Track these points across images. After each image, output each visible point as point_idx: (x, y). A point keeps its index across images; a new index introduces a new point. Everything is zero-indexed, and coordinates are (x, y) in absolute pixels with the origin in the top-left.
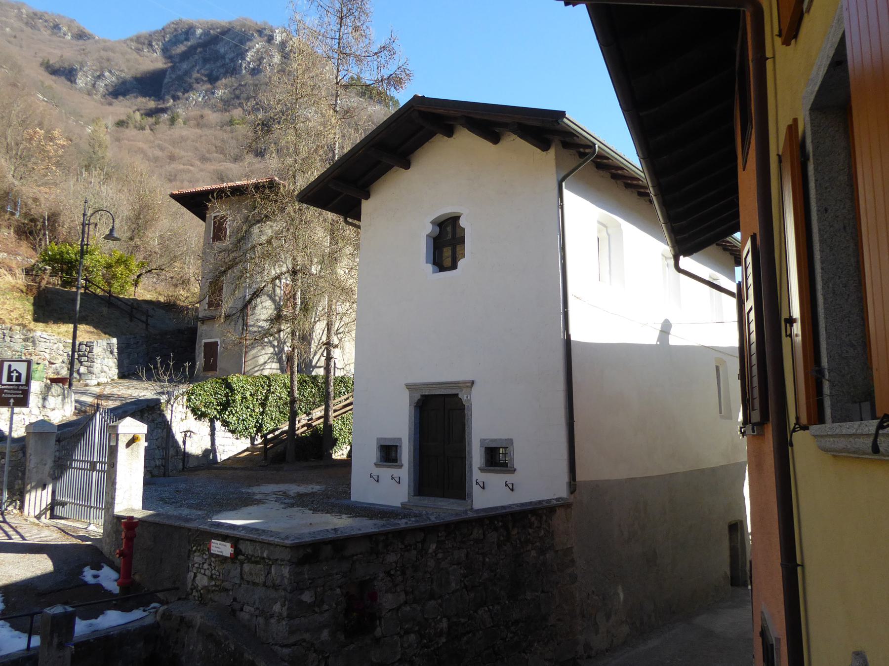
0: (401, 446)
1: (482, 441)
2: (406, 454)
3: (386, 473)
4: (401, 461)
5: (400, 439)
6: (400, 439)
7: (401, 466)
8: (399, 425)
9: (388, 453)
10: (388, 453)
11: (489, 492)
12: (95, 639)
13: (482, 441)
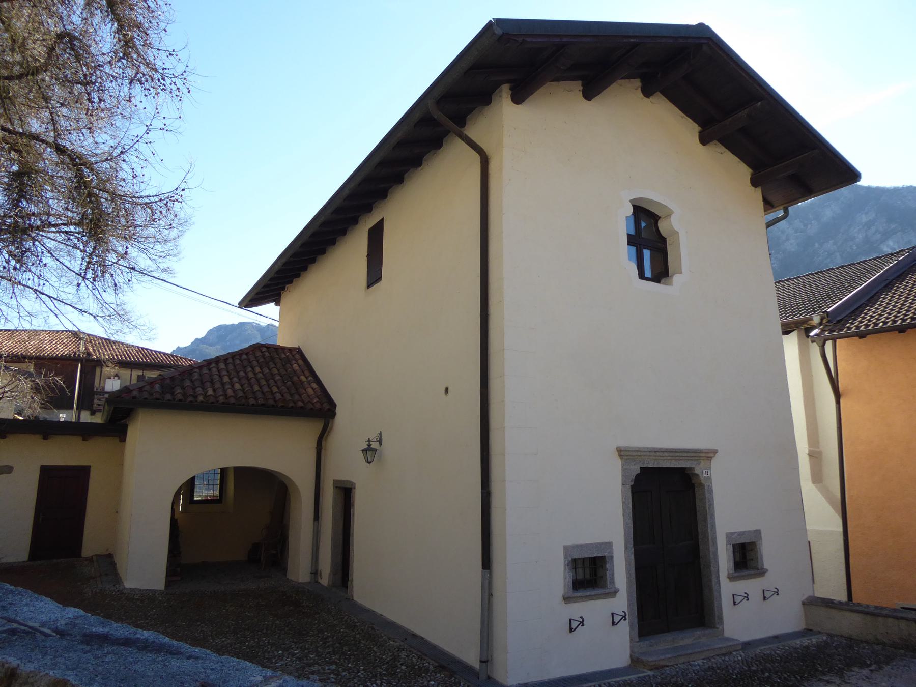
0: (612, 557)
1: (729, 536)
2: (621, 571)
3: (595, 610)
4: (613, 582)
5: (609, 545)
6: (609, 545)
7: (614, 593)
8: (607, 523)
9: (588, 573)
10: (588, 573)
11: (749, 614)
12: (311, 236)
13: (729, 536)
